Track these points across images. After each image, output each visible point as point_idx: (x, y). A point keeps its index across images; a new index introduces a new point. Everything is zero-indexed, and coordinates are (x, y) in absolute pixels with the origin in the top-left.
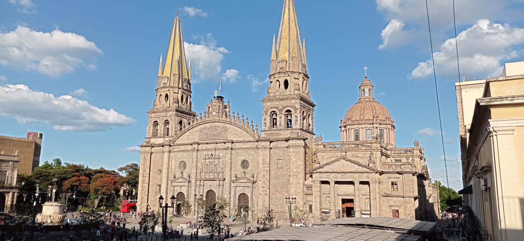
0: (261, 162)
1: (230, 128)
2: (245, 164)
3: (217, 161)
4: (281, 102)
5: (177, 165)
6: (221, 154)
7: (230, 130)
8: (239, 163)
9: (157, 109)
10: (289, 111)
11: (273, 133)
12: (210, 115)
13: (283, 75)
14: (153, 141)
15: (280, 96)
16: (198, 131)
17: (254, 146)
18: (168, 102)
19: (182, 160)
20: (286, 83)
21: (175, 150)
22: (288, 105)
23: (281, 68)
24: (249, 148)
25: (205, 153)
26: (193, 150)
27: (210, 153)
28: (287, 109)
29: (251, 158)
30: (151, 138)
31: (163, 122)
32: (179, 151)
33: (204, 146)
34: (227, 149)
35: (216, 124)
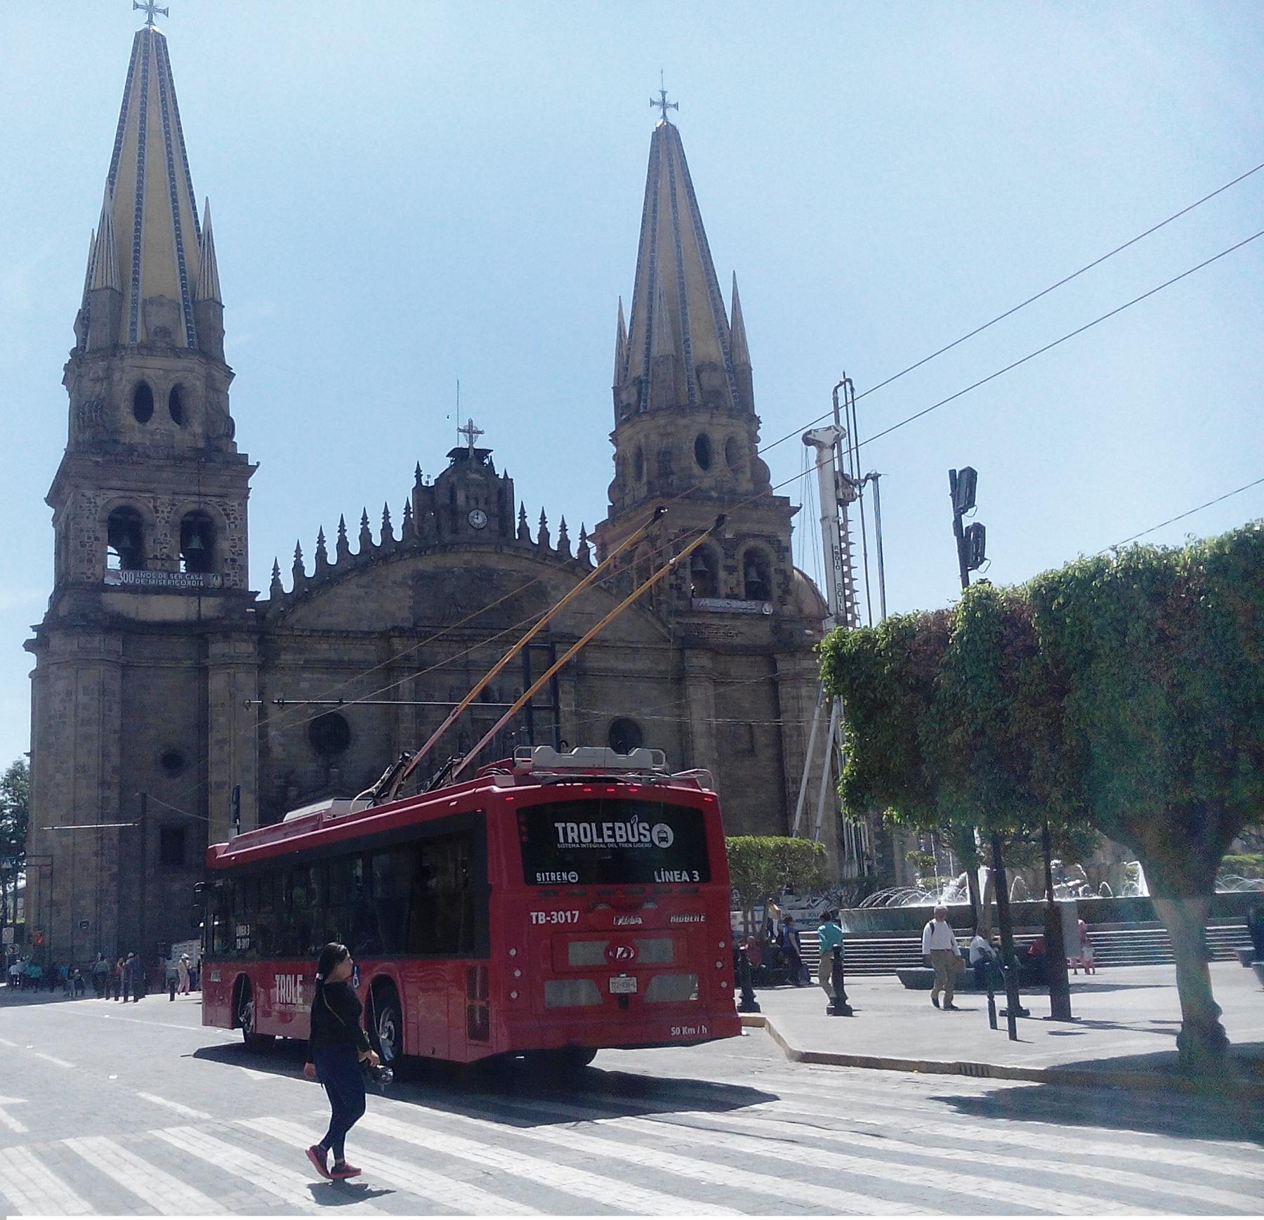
9: (131, 449)
13: (724, 420)
22: (756, 528)
28: (751, 543)
32: (308, 666)
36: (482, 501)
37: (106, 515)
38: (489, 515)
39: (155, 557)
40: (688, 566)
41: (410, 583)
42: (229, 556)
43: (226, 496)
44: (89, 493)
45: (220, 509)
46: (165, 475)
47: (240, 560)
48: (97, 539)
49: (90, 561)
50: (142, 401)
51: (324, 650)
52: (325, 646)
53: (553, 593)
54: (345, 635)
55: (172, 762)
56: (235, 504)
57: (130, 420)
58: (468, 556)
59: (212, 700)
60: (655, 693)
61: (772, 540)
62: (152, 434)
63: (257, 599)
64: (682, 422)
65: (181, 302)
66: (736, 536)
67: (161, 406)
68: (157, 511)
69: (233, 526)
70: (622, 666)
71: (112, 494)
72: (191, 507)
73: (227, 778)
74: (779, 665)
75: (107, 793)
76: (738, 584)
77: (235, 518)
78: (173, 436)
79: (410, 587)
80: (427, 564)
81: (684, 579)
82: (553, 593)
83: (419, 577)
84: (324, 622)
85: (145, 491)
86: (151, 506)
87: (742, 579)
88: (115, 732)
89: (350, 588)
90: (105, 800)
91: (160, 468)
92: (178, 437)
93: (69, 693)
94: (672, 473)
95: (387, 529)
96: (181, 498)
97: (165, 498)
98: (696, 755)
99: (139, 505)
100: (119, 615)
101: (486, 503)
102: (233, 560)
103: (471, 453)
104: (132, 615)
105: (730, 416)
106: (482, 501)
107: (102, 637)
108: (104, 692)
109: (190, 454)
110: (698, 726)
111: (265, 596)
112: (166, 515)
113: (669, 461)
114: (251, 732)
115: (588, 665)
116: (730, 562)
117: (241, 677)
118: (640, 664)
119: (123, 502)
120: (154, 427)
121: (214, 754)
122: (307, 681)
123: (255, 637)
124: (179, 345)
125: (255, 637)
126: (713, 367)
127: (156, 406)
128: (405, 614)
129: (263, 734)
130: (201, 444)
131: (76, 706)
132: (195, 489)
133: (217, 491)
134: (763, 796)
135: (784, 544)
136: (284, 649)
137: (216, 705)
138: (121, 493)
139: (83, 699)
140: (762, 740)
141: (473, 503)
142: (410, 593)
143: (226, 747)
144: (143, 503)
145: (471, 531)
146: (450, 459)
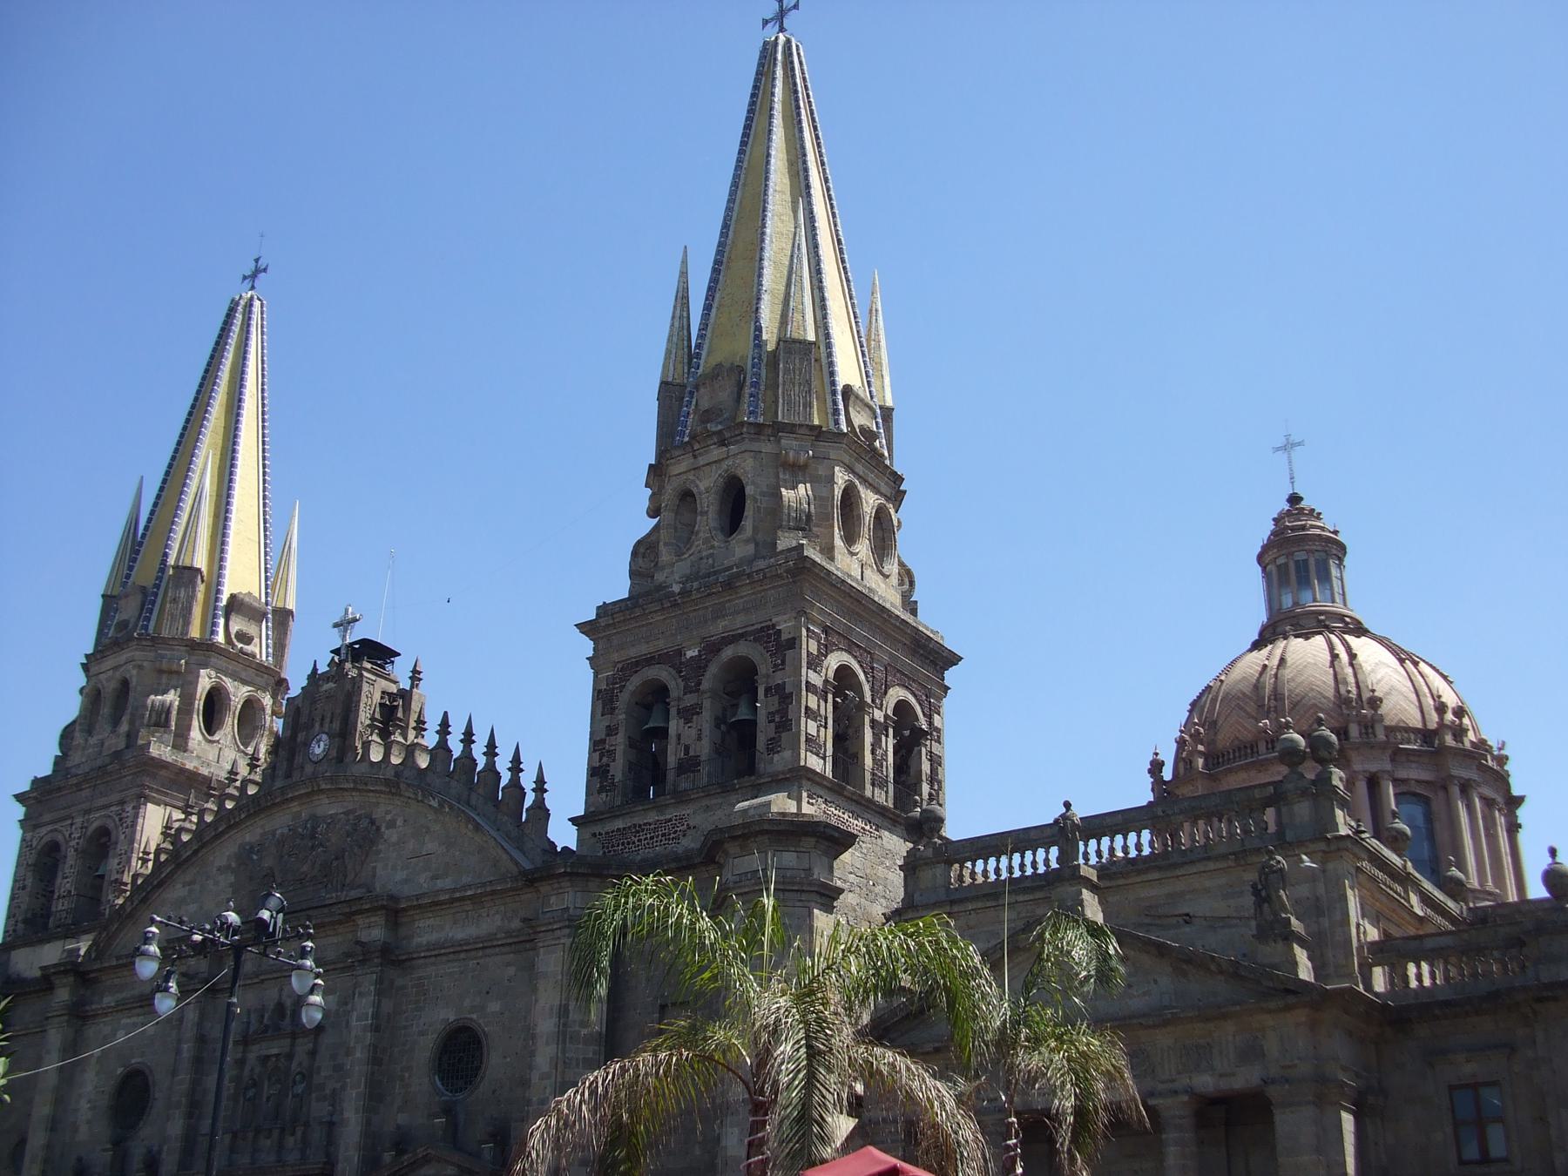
0: (546, 1026)
1: (392, 825)
2: (461, 1053)
7: (392, 835)
8: (424, 1047)
11: (639, 829)
12: (299, 759)
13: (716, 453)
15: (687, 579)
18: (124, 727)
20: (734, 498)
22: (738, 622)
23: (706, 416)
24: (485, 945)
28: (728, 653)
29: (494, 1006)
35: (328, 807)
43: (122, 803)
58: (295, 807)
60: (511, 971)
70: (460, 934)
71: (44, 830)
76: (699, 738)
80: (250, 834)
81: (611, 753)
97: (79, 820)
105: (723, 443)
115: (417, 940)
116: (690, 700)
118: (489, 922)
119: (47, 839)
134: (698, 1152)
135: (784, 637)
138: (50, 828)
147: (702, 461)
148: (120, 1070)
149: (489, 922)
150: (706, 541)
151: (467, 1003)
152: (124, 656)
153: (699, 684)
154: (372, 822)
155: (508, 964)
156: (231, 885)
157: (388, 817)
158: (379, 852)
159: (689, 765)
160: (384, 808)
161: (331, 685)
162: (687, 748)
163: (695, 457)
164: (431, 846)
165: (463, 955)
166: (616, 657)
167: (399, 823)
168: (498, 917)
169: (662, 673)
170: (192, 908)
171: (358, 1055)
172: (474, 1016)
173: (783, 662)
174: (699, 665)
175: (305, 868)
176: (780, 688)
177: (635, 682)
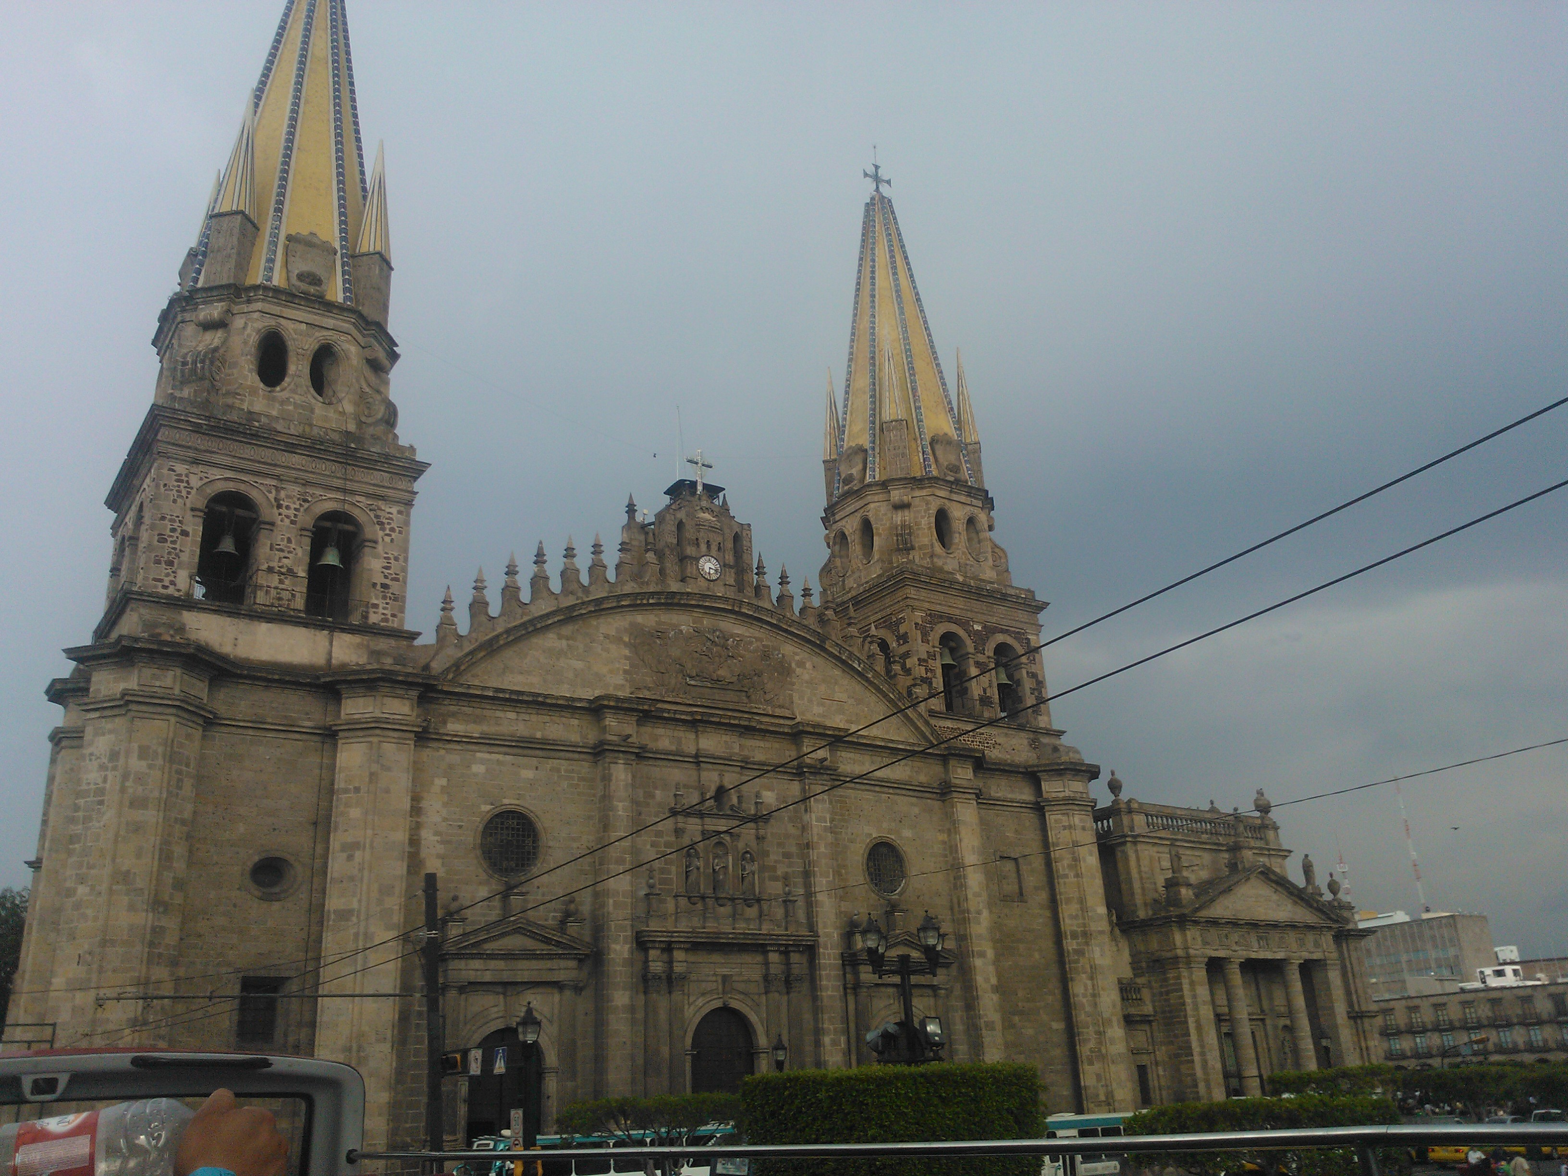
1: (801, 664)
2: (884, 861)
3: (748, 832)
4: (976, 605)
5: (470, 837)
6: (769, 797)
8: (857, 855)
10: (1002, 650)
12: (690, 570)
13: (963, 499)
14: (213, 630)
16: (619, 640)
17: (923, 778)
19: (509, 801)
21: (454, 727)
25: (677, 774)
26: (599, 752)
27: (711, 778)
28: (1000, 638)
29: (907, 833)
30: (188, 603)
31: (307, 520)
32: (488, 742)
33: (663, 738)
34: (820, 769)
36: (714, 547)
37: (201, 503)
38: (725, 565)
39: (270, 570)
40: (938, 656)
41: (626, 639)
42: (379, 579)
43: (383, 498)
44: (181, 468)
45: (372, 514)
46: (296, 460)
47: (395, 587)
48: (185, 533)
49: (170, 563)
50: (272, 360)
51: (512, 723)
52: (512, 715)
53: (798, 671)
54: (538, 703)
55: (269, 872)
56: (394, 510)
57: (252, 379)
58: (697, 614)
59: (340, 784)
60: (916, 810)
61: (1019, 636)
62: (282, 403)
63: (418, 642)
64: (917, 493)
65: (337, 246)
66: (984, 627)
67: (298, 368)
68: (279, 506)
69: (388, 539)
71: (216, 473)
72: (329, 506)
73: (355, 905)
74: (1045, 786)
75: (164, 922)
77: (392, 530)
78: (312, 411)
79: (626, 645)
80: (648, 620)
82: (798, 671)
83: (636, 630)
84: (514, 682)
85: (266, 475)
86: (272, 497)
87: (994, 680)
88: (183, 822)
89: (550, 640)
90: (157, 931)
91: (291, 448)
92: (317, 411)
93: (114, 756)
94: (913, 548)
95: (597, 568)
96: (318, 492)
98: (970, 896)
99: (254, 494)
100: (207, 644)
101: (719, 549)
102: (385, 586)
103: (700, 488)
104: (227, 649)
105: (969, 495)
106: (714, 547)
107: (179, 671)
108: (172, 757)
109: (336, 437)
110: (970, 856)
111: (428, 638)
112: (291, 512)
113: (910, 534)
114: (401, 836)
116: (981, 658)
117: (389, 748)
119: (231, 486)
120: (285, 395)
121: (337, 865)
122: (481, 764)
123: (414, 693)
124: (329, 297)
125: (414, 693)
126: (949, 442)
127: (292, 368)
128: (619, 680)
129: (414, 841)
130: (352, 427)
131: (125, 777)
132: (338, 483)
133: (371, 490)
134: (1037, 956)
136: (454, 715)
137: (346, 791)
139: (136, 764)
140: (1033, 879)
141: (703, 547)
142: (627, 652)
143: (358, 854)
144: (260, 492)
145: (703, 584)
146: (668, 497)
147: (955, 497)
148: (485, 808)
149: (900, 772)
150: (963, 553)
151: (885, 825)
152: (330, 322)
153: (984, 650)
154: (783, 656)
155: (912, 804)
156: (627, 658)
157: (797, 658)
158: (793, 684)
159: (985, 701)
160: (789, 650)
161: (707, 516)
162: (985, 690)
163: (951, 492)
164: (843, 696)
165: (877, 789)
166: (927, 605)
167: (808, 665)
168: (907, 768)
169: (961, 633)
170: (579, 665)
171: (822, 849)
172: (893, 837)
173: (1034, 660)
174: (980, 639)
175: (722, 672)
176: (1034, 676)
177: (942, 628)
